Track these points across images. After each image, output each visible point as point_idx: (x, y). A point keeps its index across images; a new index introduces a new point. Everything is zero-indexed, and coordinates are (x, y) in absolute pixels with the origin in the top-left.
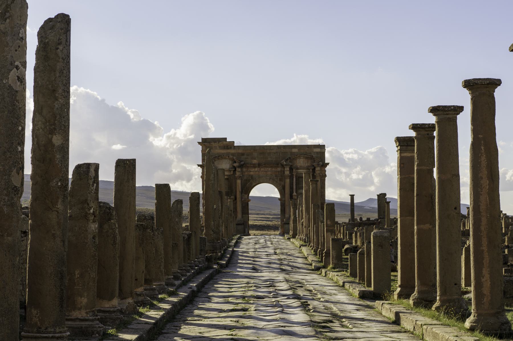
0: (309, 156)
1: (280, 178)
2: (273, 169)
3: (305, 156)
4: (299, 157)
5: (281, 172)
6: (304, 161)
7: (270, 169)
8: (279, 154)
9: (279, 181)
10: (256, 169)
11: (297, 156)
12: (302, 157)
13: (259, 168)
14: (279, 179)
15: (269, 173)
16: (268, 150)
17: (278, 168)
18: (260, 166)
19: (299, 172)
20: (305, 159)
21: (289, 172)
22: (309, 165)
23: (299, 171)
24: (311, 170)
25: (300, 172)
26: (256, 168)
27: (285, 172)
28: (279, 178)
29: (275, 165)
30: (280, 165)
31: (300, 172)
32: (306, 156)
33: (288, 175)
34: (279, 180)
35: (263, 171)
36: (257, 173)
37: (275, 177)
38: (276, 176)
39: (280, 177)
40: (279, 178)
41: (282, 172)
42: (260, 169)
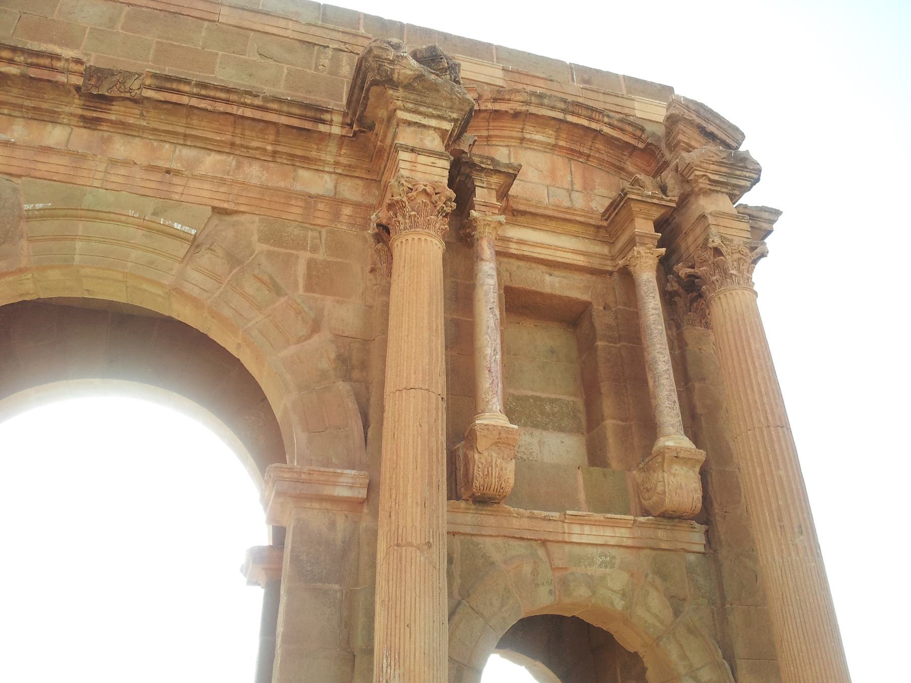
0: (607, 130)
1: (320, 256)
2: (254, 173)
3: (570, 118)
4: (516, 115)
5: (336, 216)
6: (553, 172)
7: (210, 162)
8: (327, 62)
9: (309, 288)
10: (55, 135)
11: (498, 106)
12: (538, 137)
13: (91, 123)
14: (301, 269)
15: (204, 192)
16: (224, 11)
17: (303, 174)
18: (108, 100)
19: (514, 249)
20: (560, 161)
21: (447, 164)
22: (593, 205)
23: (515, 233)
24: (644, 226)
25: (521, 242)
26: (51, 118)
27: (403, 155)
28: (304, 256)
29: (284, 120)
30: (336, 130)
31: (527, 251)
32: (585, 123)
33: (434, 185)
34: (309, 277)
35: (126, 163)
36: (56, 165)
37: (264, 239)
38: (273, 236)
39: (314, 249)
40: (304, 256)
41: (347, 211)
42: (106, 141)
